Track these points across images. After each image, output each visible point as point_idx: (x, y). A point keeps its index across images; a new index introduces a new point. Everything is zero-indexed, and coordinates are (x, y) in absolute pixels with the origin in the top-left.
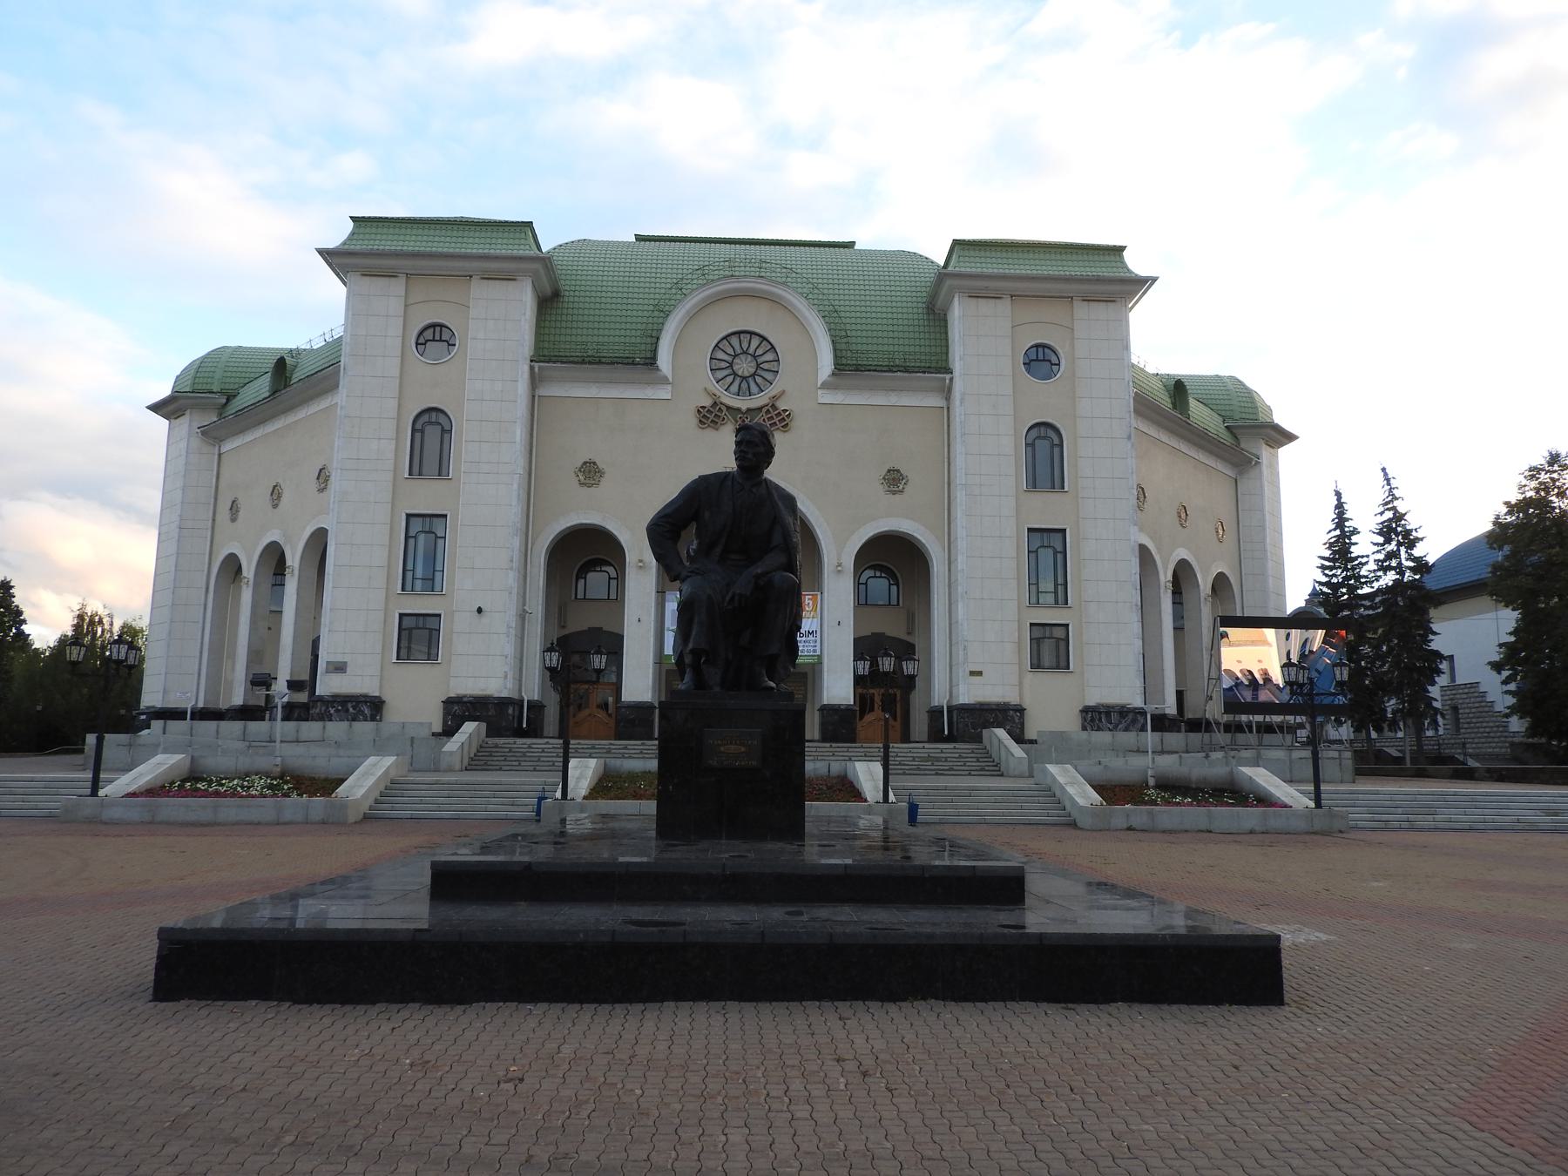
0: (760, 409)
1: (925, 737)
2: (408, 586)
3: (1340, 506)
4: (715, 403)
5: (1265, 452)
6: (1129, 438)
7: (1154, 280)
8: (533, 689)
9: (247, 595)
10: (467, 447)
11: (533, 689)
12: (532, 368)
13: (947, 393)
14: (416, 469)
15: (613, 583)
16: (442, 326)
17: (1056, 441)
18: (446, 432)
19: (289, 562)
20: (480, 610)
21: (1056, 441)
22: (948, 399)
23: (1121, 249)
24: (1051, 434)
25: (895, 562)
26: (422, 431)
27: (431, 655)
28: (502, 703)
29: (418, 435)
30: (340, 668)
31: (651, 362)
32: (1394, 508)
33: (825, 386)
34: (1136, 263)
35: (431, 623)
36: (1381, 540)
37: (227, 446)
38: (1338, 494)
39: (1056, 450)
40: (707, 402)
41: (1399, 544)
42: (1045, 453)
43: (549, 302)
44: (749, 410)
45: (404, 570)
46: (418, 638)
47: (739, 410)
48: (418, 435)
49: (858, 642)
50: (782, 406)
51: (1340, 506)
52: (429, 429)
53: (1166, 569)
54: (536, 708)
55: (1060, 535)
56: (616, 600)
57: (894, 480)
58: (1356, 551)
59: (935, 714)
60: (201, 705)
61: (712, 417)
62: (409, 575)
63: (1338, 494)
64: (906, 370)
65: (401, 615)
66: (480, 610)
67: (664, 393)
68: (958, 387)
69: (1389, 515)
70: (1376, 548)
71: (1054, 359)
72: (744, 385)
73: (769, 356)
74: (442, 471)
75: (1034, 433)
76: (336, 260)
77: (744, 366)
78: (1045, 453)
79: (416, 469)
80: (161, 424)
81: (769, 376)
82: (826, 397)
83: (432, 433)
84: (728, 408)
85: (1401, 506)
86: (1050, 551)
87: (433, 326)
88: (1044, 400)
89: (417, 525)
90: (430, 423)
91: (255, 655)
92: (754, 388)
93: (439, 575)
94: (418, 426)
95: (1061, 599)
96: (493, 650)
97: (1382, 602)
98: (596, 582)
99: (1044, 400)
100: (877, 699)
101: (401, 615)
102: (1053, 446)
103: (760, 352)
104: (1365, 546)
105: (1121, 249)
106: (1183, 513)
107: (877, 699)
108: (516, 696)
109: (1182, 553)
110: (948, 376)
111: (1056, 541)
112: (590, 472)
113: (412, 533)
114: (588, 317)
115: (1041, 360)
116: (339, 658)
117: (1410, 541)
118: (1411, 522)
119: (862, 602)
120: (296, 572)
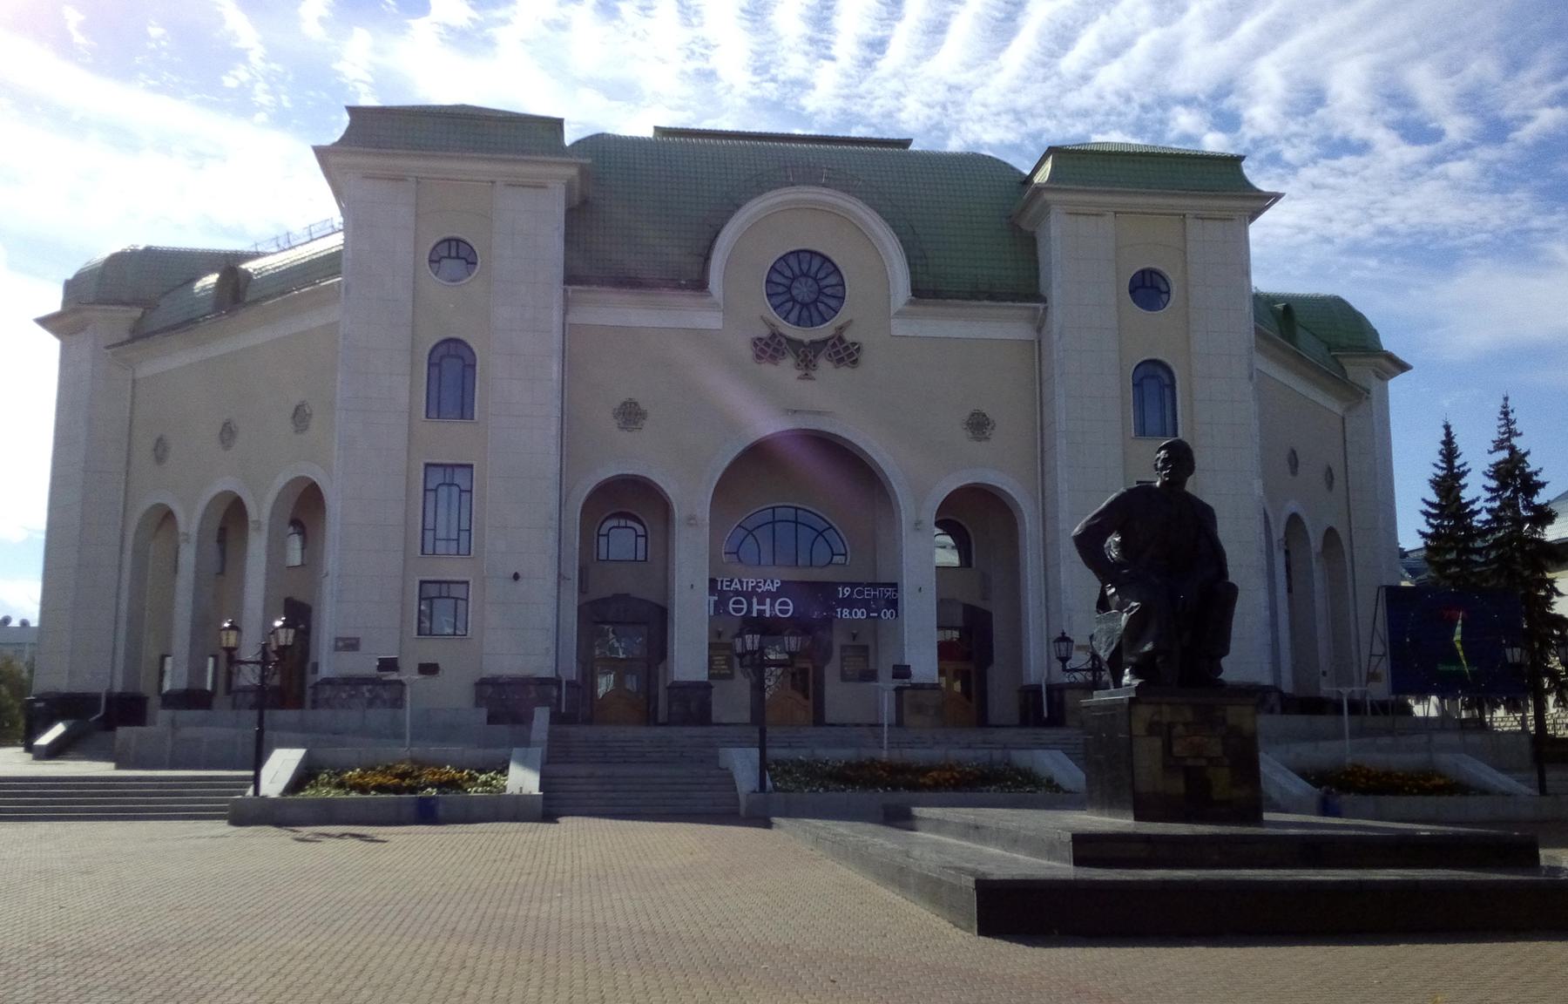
0: (825, 342)
1: (1017, 722)
2: (428, 549)
3: (1448, 442)
4: (773, 336)
5: (1374, 384)
6: (1251, 377)
9: (188, 556)
10: (497, 380)
13: (1040, 325)
15: (641, 541)
16: (458, 241)
17: (1167, 381)
19: (252, 513)
20: (516, 577)
22: (1039, 330)
24: (1160, 372)
26: (439, 365)
28: (543, 682)
29: (435, 371)
30: (351, 645)
32: (1512, 449)
33: (899, 314)
35: (458, 591)
36: (1493, 484)
37: (147, 369)
38: (1447, 427)
40: (765, 332)
41: (1516, 491)
44: (812, 342)
45: (424, 529)
47: (800, 343)
50: (849, 336)
51: (1448, 442)
57: (979, 425)
58: (1466, 495)
60: (118, 689)
61: (770, 351)
62: (429, 535)
63: (1447, 427)
64: (992, 297)
65: (422, 583)
66: (516, 577)
67: (710, 320)
68: (1057, 316)
69: (1504, 454)
70: (1488, 495)
71: (1163, 287)
73: (832, 280)
74: (464, 410)
76: (333, 160)
79: (433, 413)
81: (833, 303)
82: (899, 328)
84: (789, 340)
85: (1520, 444)
87: (449, 240)
88: (1153, 334)
89: (437, 477)
91: (203, 625)
93: (464, 535)
94: (435, 360)
97: (1498, 558)
99: (1153, 334)
101: (422, 583)
104: (1476, 490)
109: (1292, 506)
110: (1041, 306)
112: (630, 415)
113: (430, 486)
115: (1148, 289)
116: (350, 633)
117: (1530, 486)
118: (1532, 464)
120: (265, 528)
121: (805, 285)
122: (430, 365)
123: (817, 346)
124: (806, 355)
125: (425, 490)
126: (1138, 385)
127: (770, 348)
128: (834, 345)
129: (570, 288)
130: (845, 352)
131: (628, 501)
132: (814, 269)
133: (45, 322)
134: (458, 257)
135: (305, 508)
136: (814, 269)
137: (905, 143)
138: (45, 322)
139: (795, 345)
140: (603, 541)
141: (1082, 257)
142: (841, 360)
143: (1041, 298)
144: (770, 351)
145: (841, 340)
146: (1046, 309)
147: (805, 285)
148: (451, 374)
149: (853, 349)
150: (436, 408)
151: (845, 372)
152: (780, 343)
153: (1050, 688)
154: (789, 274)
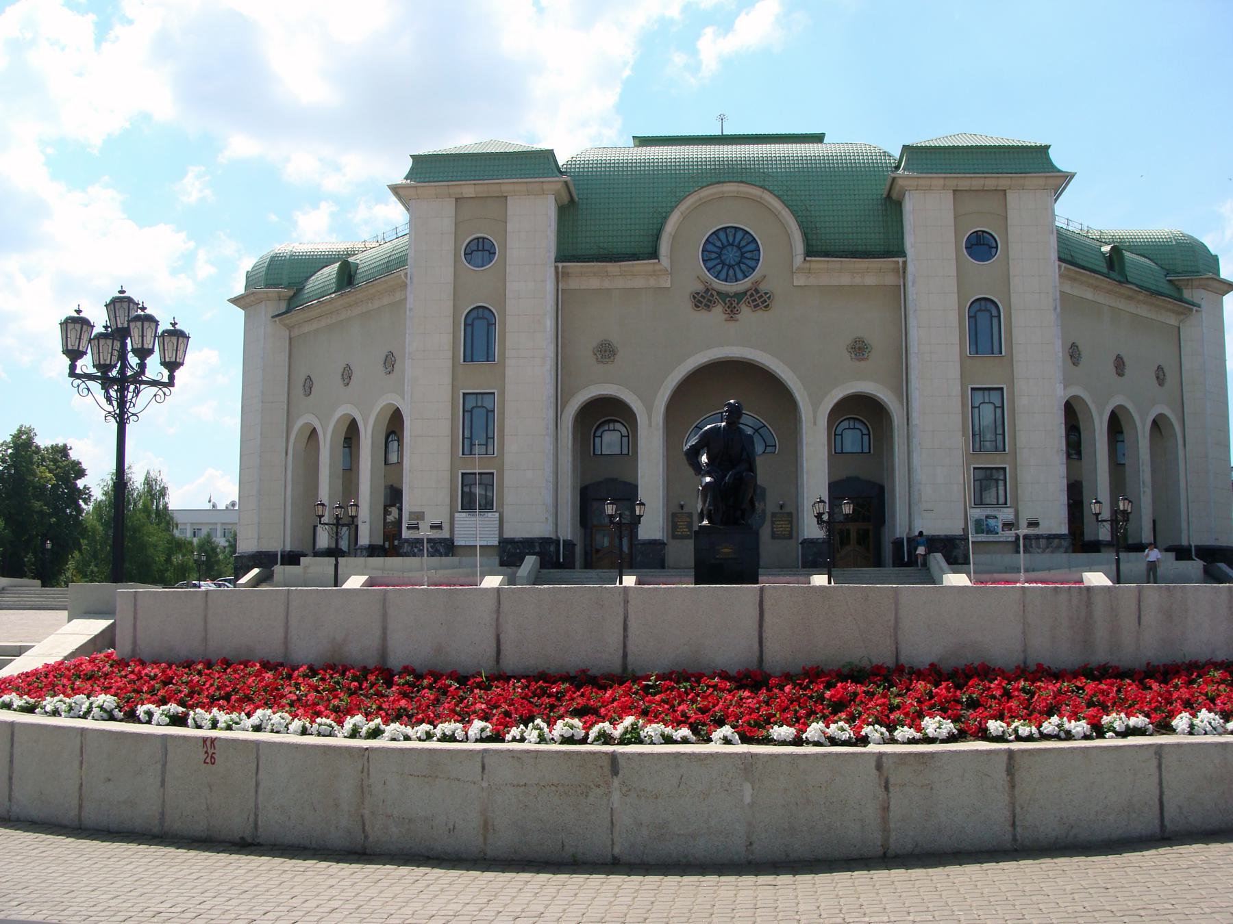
0: (745, 293)
4: (708, 290)
7: (1072, 176)
8: (567, 530)
11: (567, 530)
12: (556, 268)
14: (469, 358)
15: (625, 439)
18: (491, 325)
21: (995, 313)
23: (1047, 147)
25: (864, 416)
26: (472, 325)
27: (487, 505)
28: (545, 542)
29: (469, 329)
31: (654, 255)
34: (1059, 159)
39: (995, 321)
40: (700, 288)
42: (984, 322)
43: (568, 209)
46: (475, 493)
47: (727, 295)
48: (469, 329)
49: (830, 485)
50: (763, 287)
52: (477, 323)
53: (1101, 418)
54: (569, 545)
55: (999, 392)
56: (630, 454)
57: (859, 349)
59: (898, 544)
60: (288, 549)
61: (705, 301)
72: (731, 272)
74: (489, 357)
75: (976, 306)
77: (731, 255)
78: (984, 322)
79: (469, 358)
80: (240, 314)
83: (480, 325)
86: (991, 407)
90: (478, 318)
92: (740, 275)
94: (469, 321)
95: (1000, 448)
96: (535, 497)
98: (610, 441)
100: (853, 535)
102: (992, 317)
103: (743, 243)
105: (1047, 147)
106: (1119, 365)
107: (853, 535)
108: (553, 537)
110: (901, 260)
111: (995, 397)
112: (606, 352)
114: (602, 217)
115: (981, 245)
119: (836, 454)
121: (731, 252)
122: (465, 325)
123: (739, 296)
124: (732, 303)
125: (464, 411)
126: (973, 317)
127: (703, 300)
128: (752, 295)
129: (560, 265)
130: (759, 299)
131: (603, 414)
132: (737, 240)
133: (235, 301)
134: (483, 250)
135: (394, 426)
136: (737, 240)
137: (818, 138)
138: (235, 301)
139: (723, 296)
140: (598, 440)
141: (930, 224)
142: (755, 306)
143: (902, 253)
144: (705, 301)
145: (757, 291)
146: (905, 263)
147: (731, 252)
148: (479, 332)
149: (765, 297)
150: (469, 357)
151: (761, 315)
152: (712, 295)
153: (908, 539)
154: (719, 244)
